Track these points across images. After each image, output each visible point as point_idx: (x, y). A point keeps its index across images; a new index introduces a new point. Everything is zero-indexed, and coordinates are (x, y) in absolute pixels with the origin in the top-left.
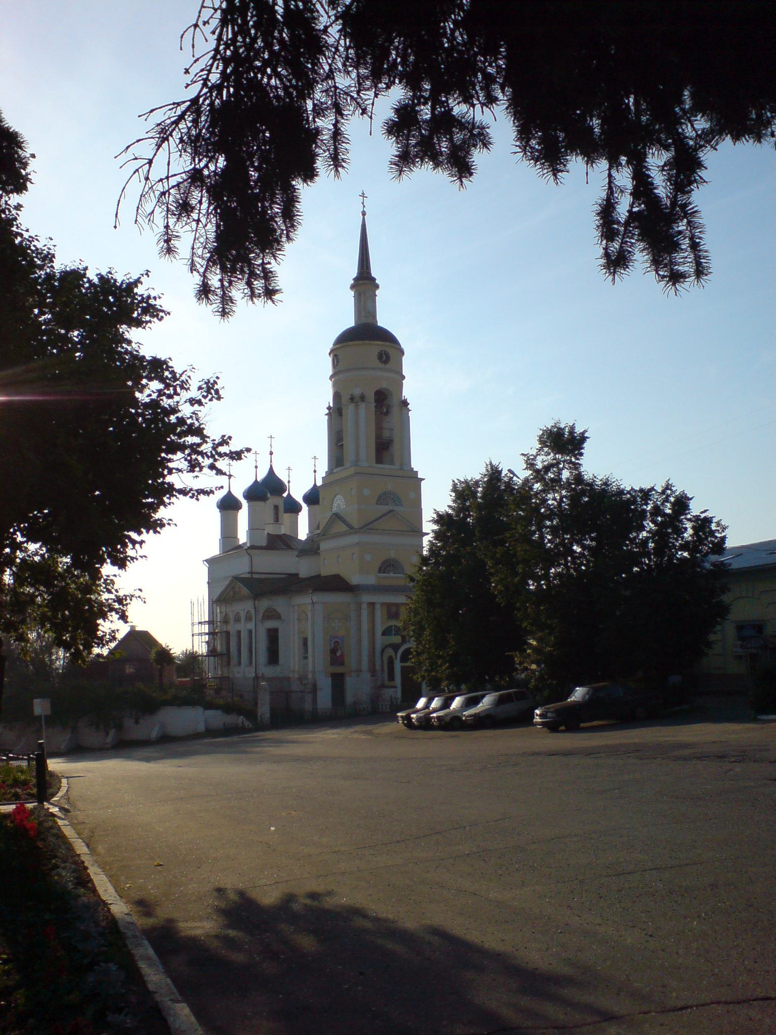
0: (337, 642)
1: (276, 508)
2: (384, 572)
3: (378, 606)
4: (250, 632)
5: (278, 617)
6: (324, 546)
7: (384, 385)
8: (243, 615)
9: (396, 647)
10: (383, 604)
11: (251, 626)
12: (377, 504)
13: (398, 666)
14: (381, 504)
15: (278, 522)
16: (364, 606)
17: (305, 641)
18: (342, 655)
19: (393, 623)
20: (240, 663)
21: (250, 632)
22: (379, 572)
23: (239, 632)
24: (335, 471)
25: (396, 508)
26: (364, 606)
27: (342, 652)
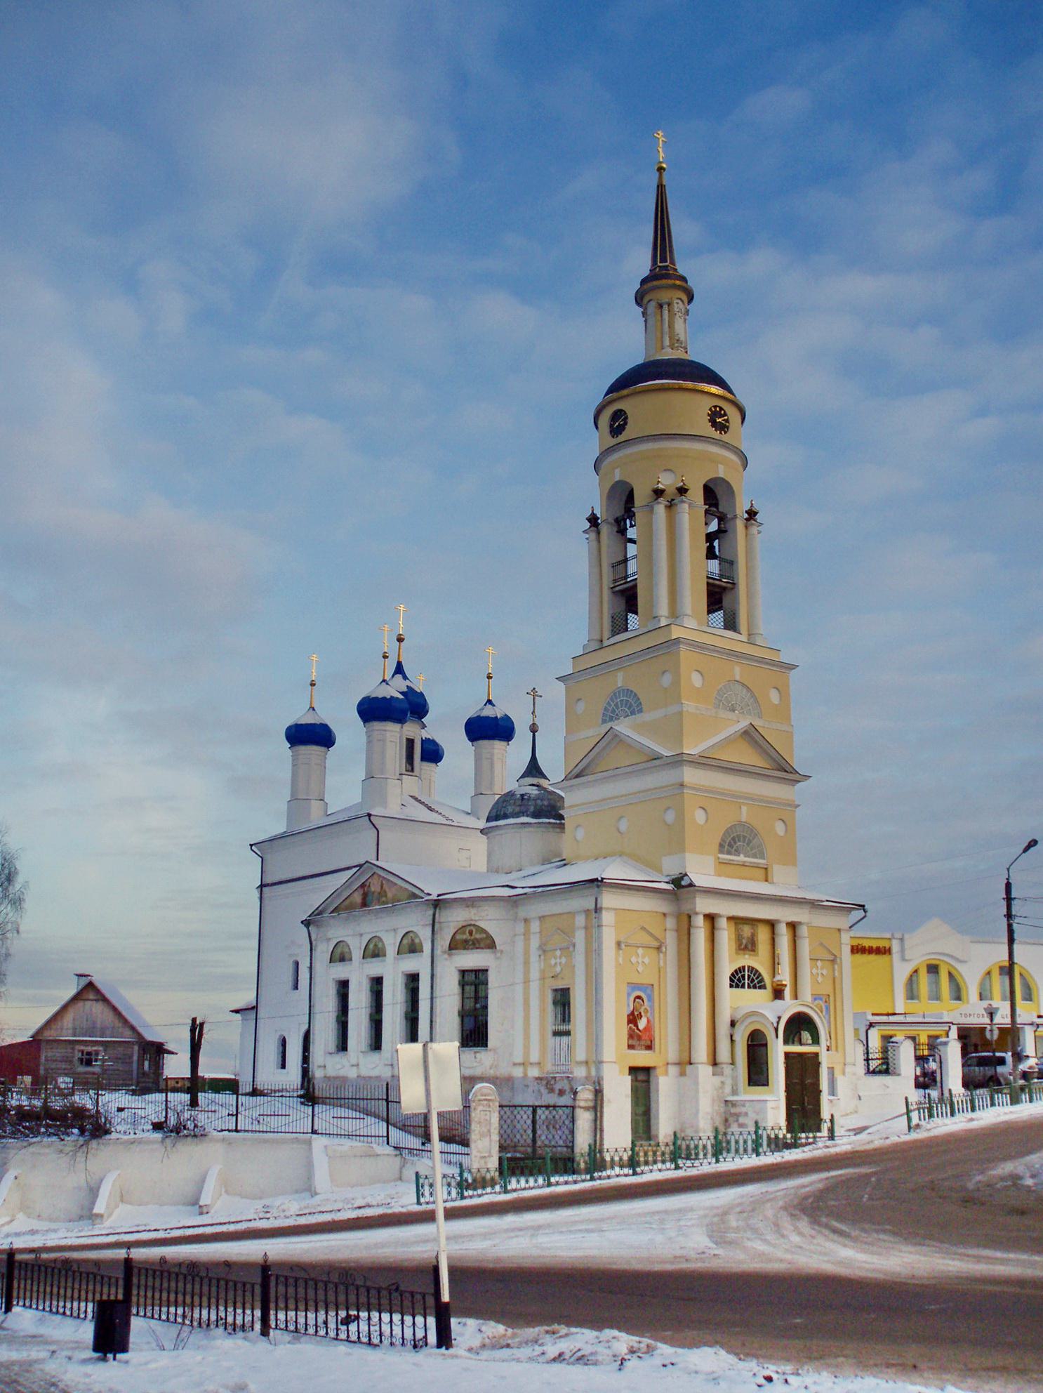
0: (639, 997)
2: (729, 853)
3: (722, 923)
5: (489, 944)
7: (721, 472)
8: (391, 943)
10: (730, 919)
18: (649, 1028)
19: (746, 961)
21: (413, 979)
22: (721, 852)
26: (699, 921)
27: (648, 1021)
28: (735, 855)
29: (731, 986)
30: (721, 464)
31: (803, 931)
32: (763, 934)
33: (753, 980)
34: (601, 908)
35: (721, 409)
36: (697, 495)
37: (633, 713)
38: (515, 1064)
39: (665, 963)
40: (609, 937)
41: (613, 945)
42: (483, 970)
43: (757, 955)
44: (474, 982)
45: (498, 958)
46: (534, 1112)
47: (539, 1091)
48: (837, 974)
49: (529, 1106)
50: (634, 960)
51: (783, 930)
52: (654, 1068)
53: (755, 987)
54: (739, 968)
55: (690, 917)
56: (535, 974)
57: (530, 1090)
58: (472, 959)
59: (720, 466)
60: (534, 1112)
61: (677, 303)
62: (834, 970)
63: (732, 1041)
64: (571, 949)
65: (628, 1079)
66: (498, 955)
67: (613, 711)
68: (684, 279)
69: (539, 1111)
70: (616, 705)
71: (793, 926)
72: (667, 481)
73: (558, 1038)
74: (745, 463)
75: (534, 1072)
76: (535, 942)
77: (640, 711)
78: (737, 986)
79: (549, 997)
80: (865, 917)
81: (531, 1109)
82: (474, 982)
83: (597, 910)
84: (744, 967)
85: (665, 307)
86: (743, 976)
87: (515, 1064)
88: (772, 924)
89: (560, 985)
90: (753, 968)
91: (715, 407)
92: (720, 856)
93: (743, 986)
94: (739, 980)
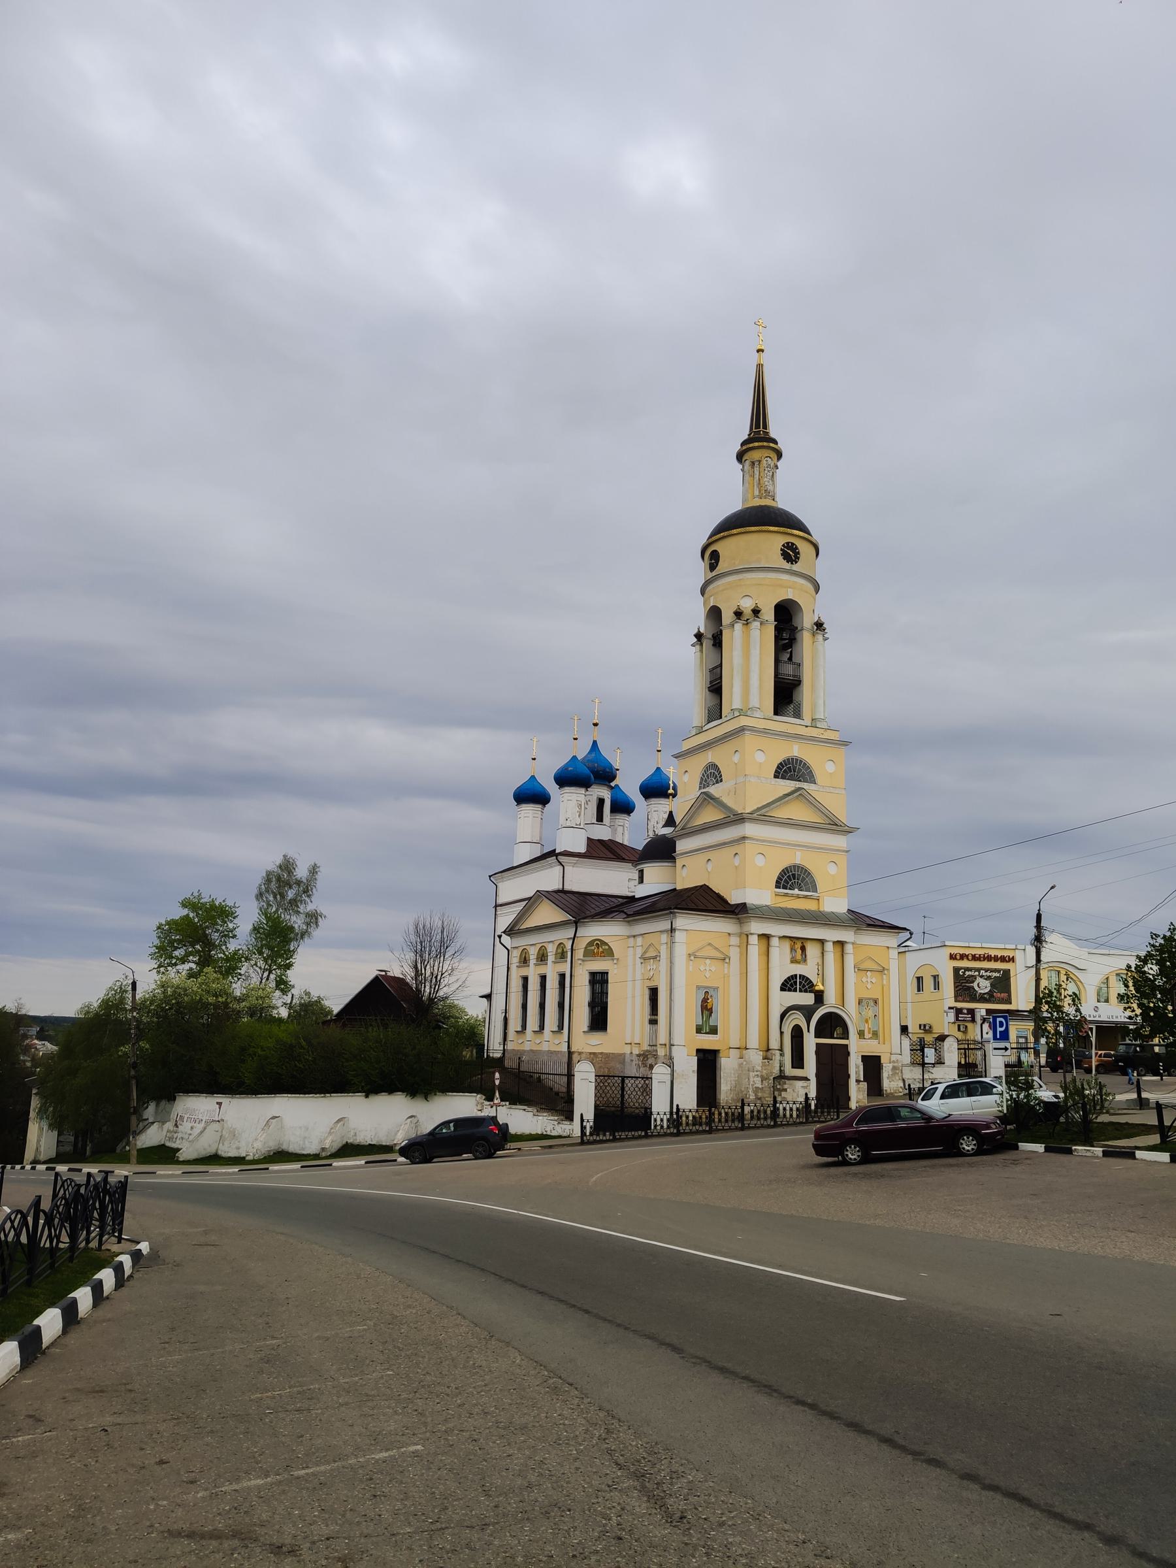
1: (601, 802)
2: (785, 888)
3: (775, 942)
4: (562, 976)
6: (681, 846)
7: (790, 595)
9: (808, 1012)
11: (565, 968)
12: (776, 777)
13: (810, 1042)
14: (783, 778)
15: (602, 821)
16: (754, 940)
17: (654, 993)
19: (798, 969)
20: (542, 1027)
22: (777, 887)
23: (543, 978)
24: (704, 729)
25: (805, 785)
26: (754, 940)
28: (790, 889)
29: (782, 989)
30: (790, 588)
31: (849, 948)
32: (812, 951)
33: (804, 986)
34: (675, 929)
35: (793, 544)
36: (769, 614)
37: (717, 782)
38: (626, 1044)
39: (729, 972)
40: (681, 951)
41: (685, 957)
42: (605, 973)
43: (807, 964)
44: (599, 981)
45: (615, 964)
46: (623, 1081)
47: (639, 1064)
48: (885, 982)
49: (619, 1077)
50: (702, 968)
51: (829, 947)
52: (719, 1050)
53: (806, 991)
54: (792, 976)
55: (747, 935)
56: (638, 976)
57: (634, 1063)
58: (598, 966)
59: (789, 590)
60: (623, 1081)
61: (767, 461)
62: (882, 979)
63: (782, 1033)
64: (658, 959)
65: (694, 1060)
66: (615, 961)
67: (706, 781)
68: (775, 442)
69: (627, 1081)
70: (708, 776)
71: (841, 944)
72: (747, 605)
73: (652, 1026)
74: (817, 588)
75: (636, 1051)
76: (639, 951)
77: (721, 781)
78: (790, 990)
79: (647, 993)
80: (911, 938)
81: (620, 1078)
82: (599, 981)
83: (672, 930)
84: (796, 975)
85: (756, 463)
86: (795, 983)
87: (626, 1044)
88: (822, 942)
89: (652, 984)
90: (804, 976)
91: (788, 543)
92: (778, 890)
93: (795, 990)
94: (791, 985)
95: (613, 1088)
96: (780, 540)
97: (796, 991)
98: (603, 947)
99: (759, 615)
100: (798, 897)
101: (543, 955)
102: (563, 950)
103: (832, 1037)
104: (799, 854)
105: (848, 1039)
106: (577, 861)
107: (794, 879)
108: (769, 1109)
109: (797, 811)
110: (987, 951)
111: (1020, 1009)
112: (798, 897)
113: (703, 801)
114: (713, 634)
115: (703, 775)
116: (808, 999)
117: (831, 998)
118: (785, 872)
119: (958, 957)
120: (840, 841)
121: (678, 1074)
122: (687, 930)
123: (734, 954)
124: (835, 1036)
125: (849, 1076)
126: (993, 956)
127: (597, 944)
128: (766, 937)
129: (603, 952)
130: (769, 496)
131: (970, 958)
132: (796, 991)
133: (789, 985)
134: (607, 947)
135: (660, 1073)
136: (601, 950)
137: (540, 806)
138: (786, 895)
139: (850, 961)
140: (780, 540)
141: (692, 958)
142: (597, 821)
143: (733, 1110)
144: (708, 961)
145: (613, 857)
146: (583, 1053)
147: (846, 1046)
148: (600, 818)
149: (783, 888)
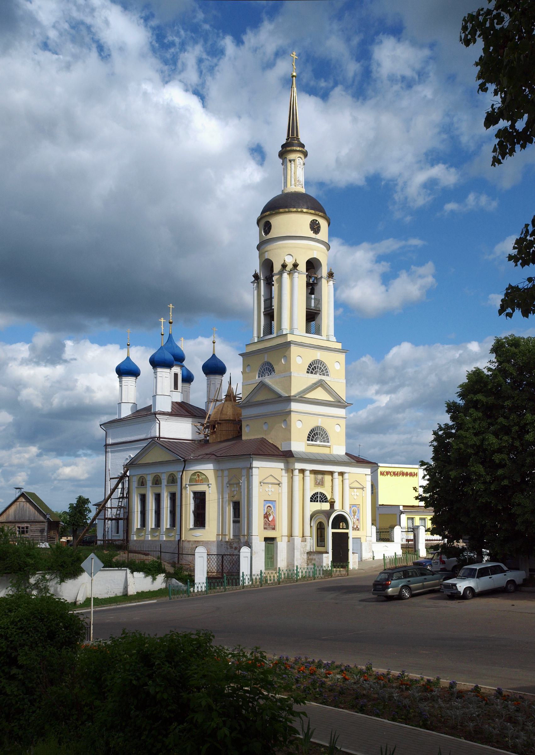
2: (312, 440)
3: (307, 473)
9: (327, 514)
13: (330, 531)
16: (296, 472)
19: (319, 490)
28: (315, 441)
33: (322, 499)
51: (336, 475)
54: (316, 493)
71: (342, 474)
78: (314, 501)
84: (318, 493)
86: (317, 497)
88: (331, 473)
93: (317, 501)
95: (211, 561)
96: (310, 218)
97: (318, 502)
98: (202, 477)
99: (298, 268)
100: (319, 446)
101: (157, 481)
102: (173, 478)
103: (339, 528)
104: (320, 420)
105: (348, 529)
106: (168, 418)
107: (317, 435)
108: (304, 570)
109: (320, 394)
110: (402, 469)
111: (420, 505)
112: (319, 446)
113: (262, 386)
114: (266, 277)
115: (261, 368)
116: (326, 506)
117: (337, 506)
118: (312, 431)
119: (385, 474)
120: (341, 412)
121: (254, 552)
122: (259, 468)
123: (285, 480)
124: (341, 527)
125: (348, 550)
126: (405, 472)
127: (198, 475)
128: (302, 471)
129: (202, 480)
130: (300, 185)
131: (392, 474)
132: (318, 502)
133: (314, 498)
134: (204, 477)
135: (244, 551)
136: (200, 478)
137: (135, 378)
138: (313, 445)
139: (347, 483)
140: (310, 218)
141: (262, 484)
142: (174, 389)
143: (292, 572)
144: (270, 486)
145: (188, 414)
146: (190, 541)
147: (347, 533)
148: (176, 387)
149: (311, 441)
